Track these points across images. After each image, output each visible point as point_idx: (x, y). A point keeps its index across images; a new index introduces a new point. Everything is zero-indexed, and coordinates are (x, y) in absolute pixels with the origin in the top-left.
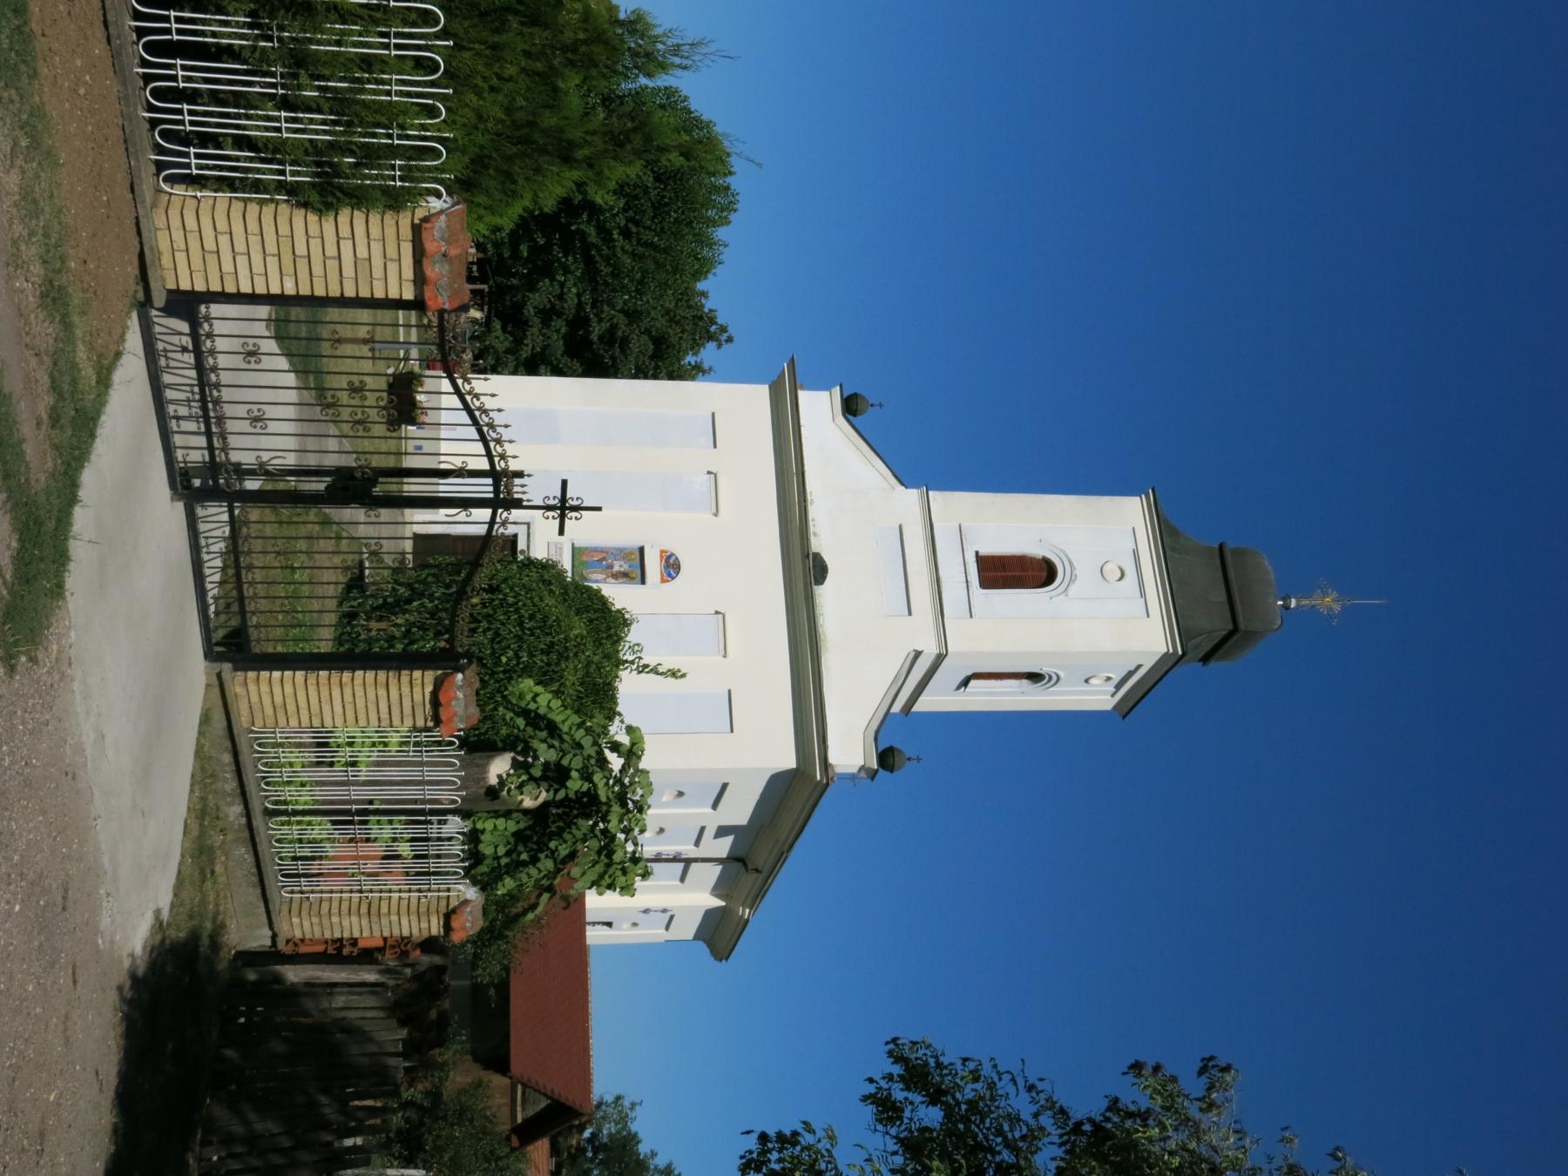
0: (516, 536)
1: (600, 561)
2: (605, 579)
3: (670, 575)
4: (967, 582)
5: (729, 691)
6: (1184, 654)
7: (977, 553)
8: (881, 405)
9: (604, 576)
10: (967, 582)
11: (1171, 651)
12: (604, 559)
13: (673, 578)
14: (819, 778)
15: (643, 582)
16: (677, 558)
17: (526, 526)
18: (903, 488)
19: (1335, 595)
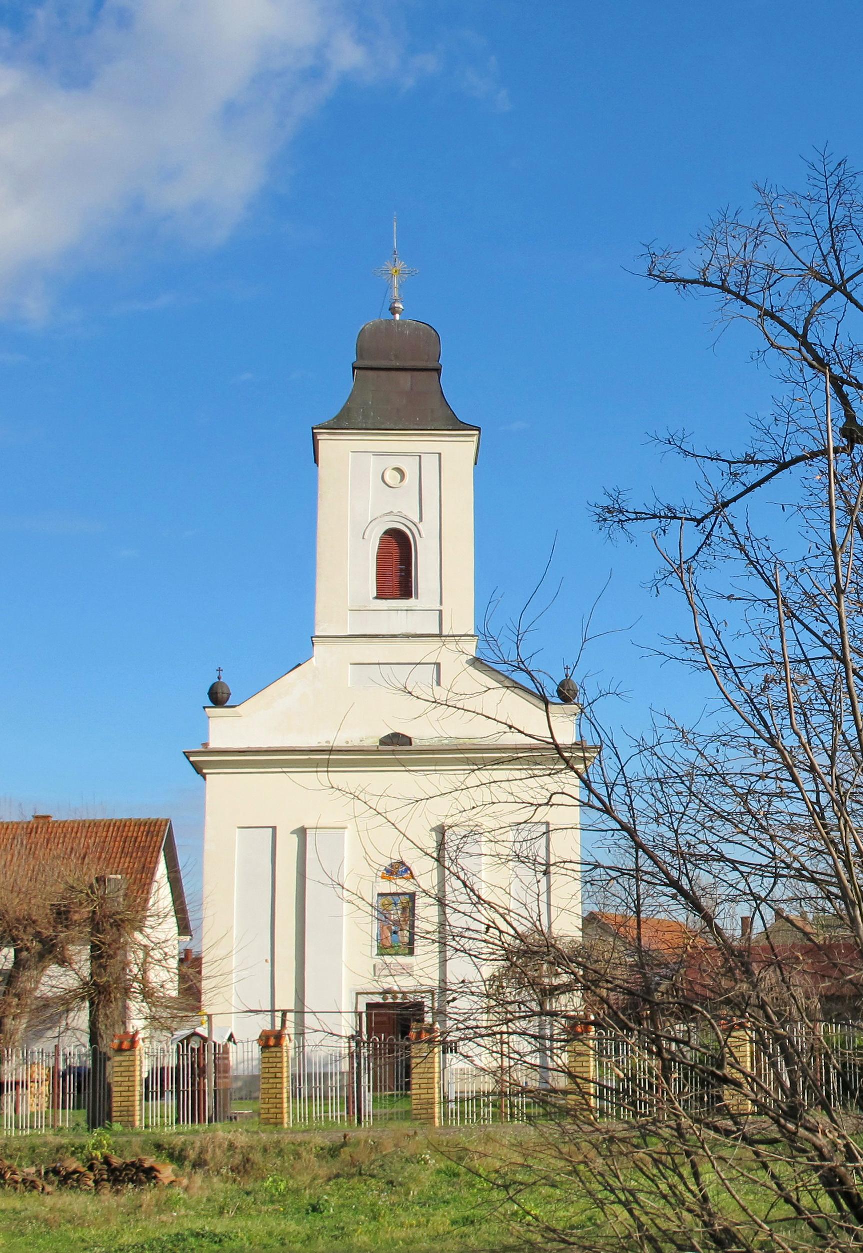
3: (406, 871)
7: (377, 598)
13: (409, 869)
18: (314, 659)
19: (389, 265)
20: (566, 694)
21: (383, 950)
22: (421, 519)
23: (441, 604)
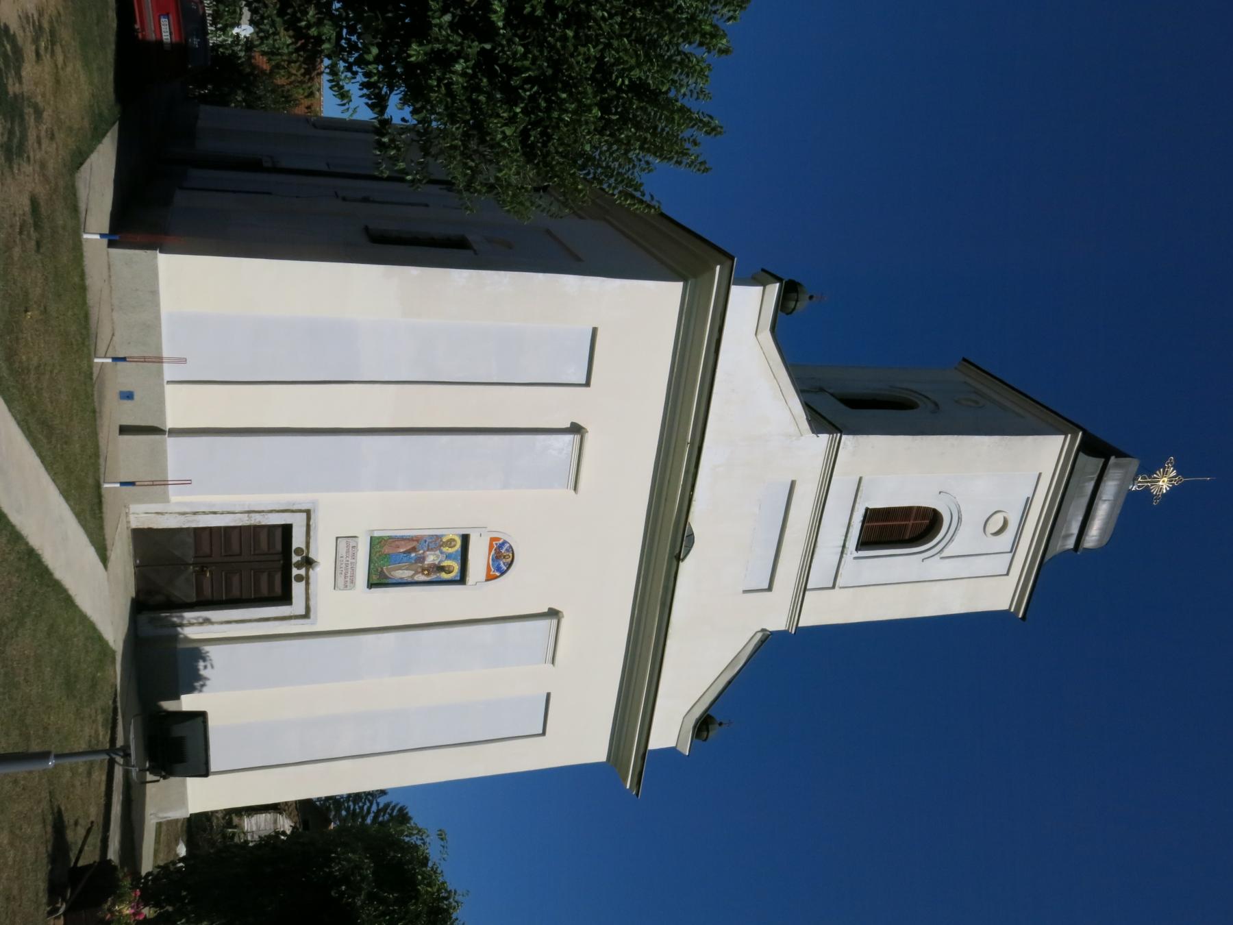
0: (287, 530)
1: (408, 552)
3: (498, 569)
4: (844, 546)
5: (548, 695)
6: (1024, 617)
9: (412, 573)
10: (844, 546)
11: (1012, 610)
12: (414, 549)
13: (503, 573)
14: (628, 787)
15: (462, 580)
16: (511, 547)
17: (304, 515)
21: (376, 543)
22: (942, 558)
23: (841, 588)
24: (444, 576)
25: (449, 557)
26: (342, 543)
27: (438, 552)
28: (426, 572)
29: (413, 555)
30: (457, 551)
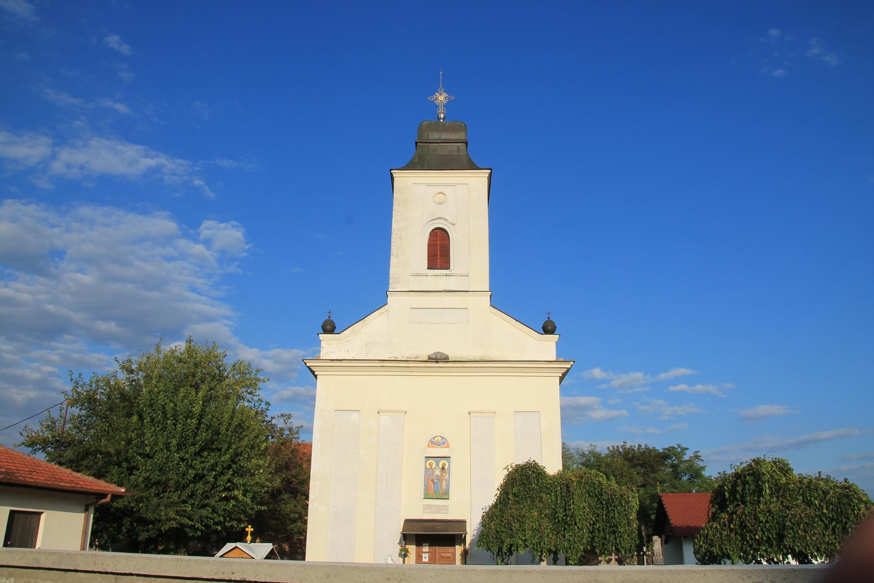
2: (445, 480)
6: (491, 169)
7: (428, 269)
8: (330, 312)
12: (433, 481)
15: (447, 458)
19: (437, 94)
20: (548, 329)
24: (446, 467)
25: (437, 465)
26: (426, 510)
27: (435, 470)
28: (444, 474)
29: (435, 481)
30: (435, 461)
